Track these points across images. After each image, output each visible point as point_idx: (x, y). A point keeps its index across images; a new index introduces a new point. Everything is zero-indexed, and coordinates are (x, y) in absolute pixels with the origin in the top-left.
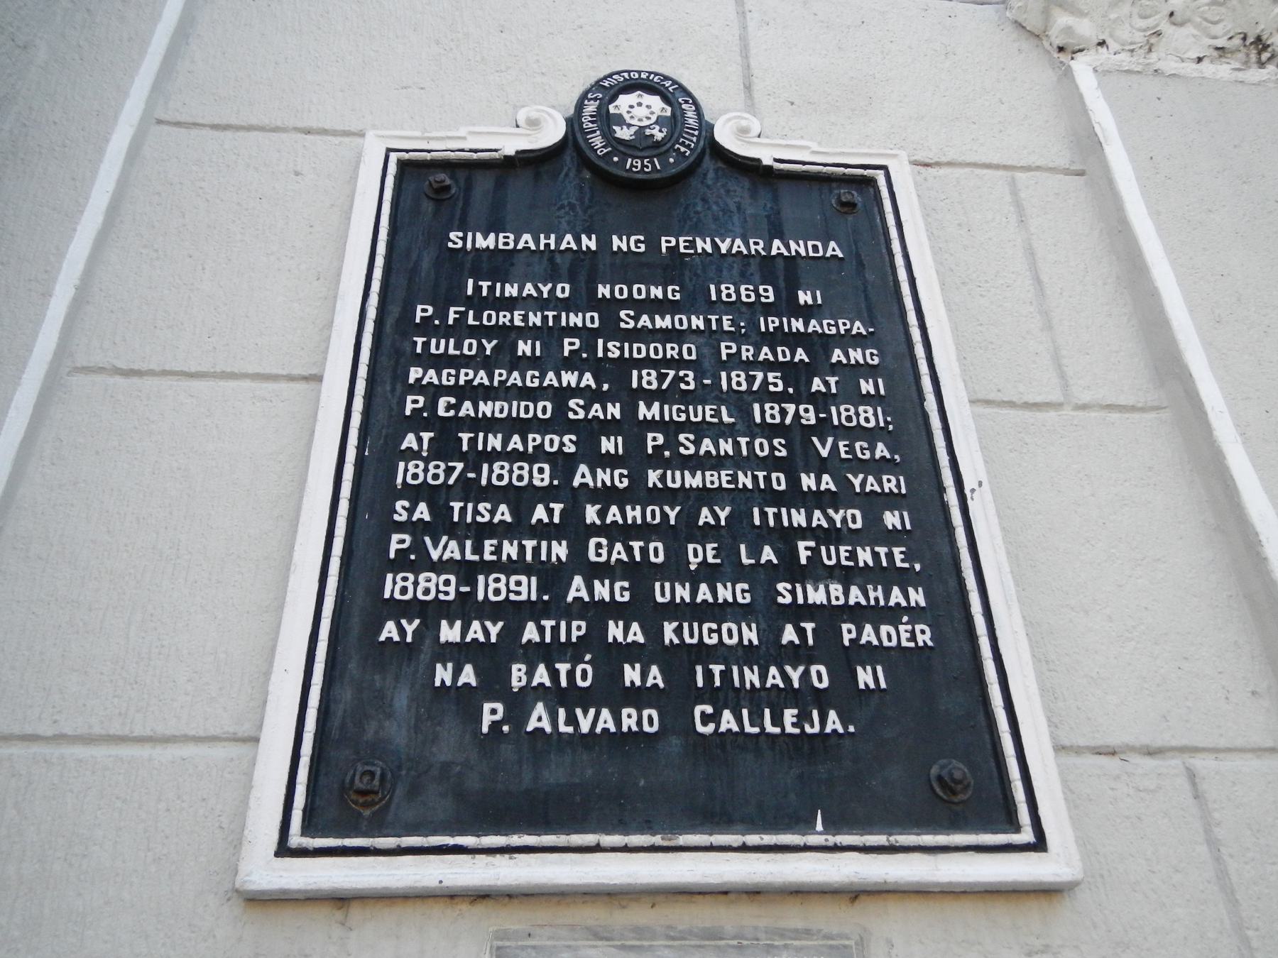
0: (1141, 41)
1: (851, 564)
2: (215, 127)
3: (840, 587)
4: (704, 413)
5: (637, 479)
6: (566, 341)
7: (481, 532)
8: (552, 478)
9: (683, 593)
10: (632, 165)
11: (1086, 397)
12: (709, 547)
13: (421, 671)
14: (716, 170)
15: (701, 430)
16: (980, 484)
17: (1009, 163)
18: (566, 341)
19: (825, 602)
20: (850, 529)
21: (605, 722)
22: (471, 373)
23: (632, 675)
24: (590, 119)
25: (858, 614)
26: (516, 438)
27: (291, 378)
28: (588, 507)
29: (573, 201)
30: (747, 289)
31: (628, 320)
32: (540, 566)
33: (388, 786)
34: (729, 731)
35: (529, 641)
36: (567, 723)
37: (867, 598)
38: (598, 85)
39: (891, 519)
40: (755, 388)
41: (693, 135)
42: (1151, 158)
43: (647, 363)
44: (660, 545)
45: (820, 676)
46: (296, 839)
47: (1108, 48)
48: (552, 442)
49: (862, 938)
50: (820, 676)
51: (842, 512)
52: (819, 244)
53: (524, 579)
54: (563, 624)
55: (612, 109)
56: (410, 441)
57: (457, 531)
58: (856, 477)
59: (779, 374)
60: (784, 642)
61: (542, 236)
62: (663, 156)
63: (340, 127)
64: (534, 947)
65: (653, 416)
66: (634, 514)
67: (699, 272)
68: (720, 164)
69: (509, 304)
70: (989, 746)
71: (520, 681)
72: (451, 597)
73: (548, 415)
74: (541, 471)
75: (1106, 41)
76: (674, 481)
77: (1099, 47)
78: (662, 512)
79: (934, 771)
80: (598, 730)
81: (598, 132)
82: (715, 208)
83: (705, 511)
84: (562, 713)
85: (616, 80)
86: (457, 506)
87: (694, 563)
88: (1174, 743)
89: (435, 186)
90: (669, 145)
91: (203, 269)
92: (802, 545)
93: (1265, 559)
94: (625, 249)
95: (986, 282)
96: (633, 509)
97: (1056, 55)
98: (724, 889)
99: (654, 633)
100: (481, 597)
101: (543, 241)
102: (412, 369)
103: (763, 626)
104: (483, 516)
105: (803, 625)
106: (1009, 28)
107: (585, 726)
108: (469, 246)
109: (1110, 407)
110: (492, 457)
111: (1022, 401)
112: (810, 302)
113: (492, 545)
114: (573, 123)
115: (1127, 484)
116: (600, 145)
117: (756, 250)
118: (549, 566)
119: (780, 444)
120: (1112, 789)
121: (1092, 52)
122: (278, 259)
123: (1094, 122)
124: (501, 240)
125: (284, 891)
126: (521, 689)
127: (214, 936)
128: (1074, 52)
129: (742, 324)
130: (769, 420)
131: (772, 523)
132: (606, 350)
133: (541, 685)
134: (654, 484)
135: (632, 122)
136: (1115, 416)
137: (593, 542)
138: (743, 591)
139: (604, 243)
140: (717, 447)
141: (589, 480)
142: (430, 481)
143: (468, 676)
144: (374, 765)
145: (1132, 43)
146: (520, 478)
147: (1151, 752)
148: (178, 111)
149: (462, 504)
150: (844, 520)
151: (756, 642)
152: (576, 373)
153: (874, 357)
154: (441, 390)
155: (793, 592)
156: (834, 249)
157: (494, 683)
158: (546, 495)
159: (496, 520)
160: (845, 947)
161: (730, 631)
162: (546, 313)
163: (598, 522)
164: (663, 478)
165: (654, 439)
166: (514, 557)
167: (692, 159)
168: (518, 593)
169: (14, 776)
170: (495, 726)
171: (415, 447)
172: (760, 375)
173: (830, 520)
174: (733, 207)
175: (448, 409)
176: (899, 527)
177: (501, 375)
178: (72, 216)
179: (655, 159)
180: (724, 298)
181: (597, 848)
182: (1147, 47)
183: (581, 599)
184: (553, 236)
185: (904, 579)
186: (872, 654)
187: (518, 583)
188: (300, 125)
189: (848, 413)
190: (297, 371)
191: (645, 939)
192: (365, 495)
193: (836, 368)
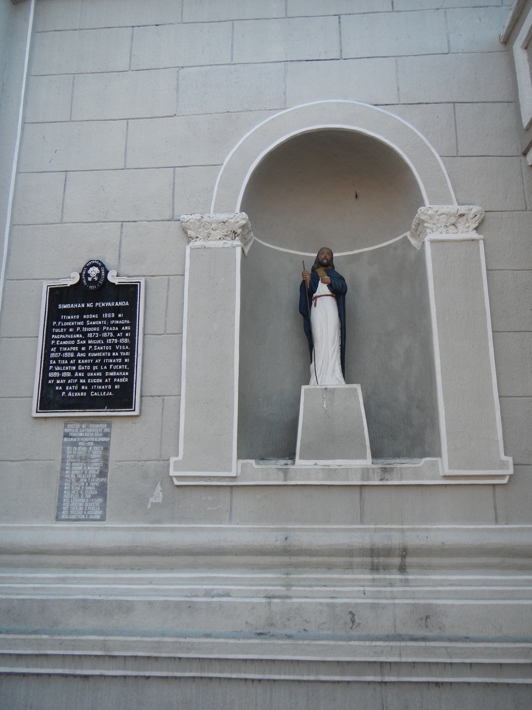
3: (115, 373)
4: (99, 342)
5: (87, 355)
8: (74, 355)
9: (92, 374)
15: (98, 345)
25: (117, 377)
45: (110, 387)
46: (38, 411)
50: (110, 387)
54: (74, 380)
56: (52, 350)
66: (86, 361)
74: (72, 354)
78: (90, 360)
83: (97, 360)
84: (73, 393)
86: (59, 361)
92: (111, 365)
99: (87, 381)
102: (53, 335)
107: (76, 395)
108: (62, 308)
110: (65, 352)
132: (84, 329)
139: (86, 305)
143: (61, 388)
146: (69, 355)
150: (118, 361)
154: (58, 339)
156: (127, 304)
157: (64, 389)
164: (91, 355)
165: (90, 347)
168: (68, 375)
170: (64, 395)
186: (117, 383)
187: (68, 374)
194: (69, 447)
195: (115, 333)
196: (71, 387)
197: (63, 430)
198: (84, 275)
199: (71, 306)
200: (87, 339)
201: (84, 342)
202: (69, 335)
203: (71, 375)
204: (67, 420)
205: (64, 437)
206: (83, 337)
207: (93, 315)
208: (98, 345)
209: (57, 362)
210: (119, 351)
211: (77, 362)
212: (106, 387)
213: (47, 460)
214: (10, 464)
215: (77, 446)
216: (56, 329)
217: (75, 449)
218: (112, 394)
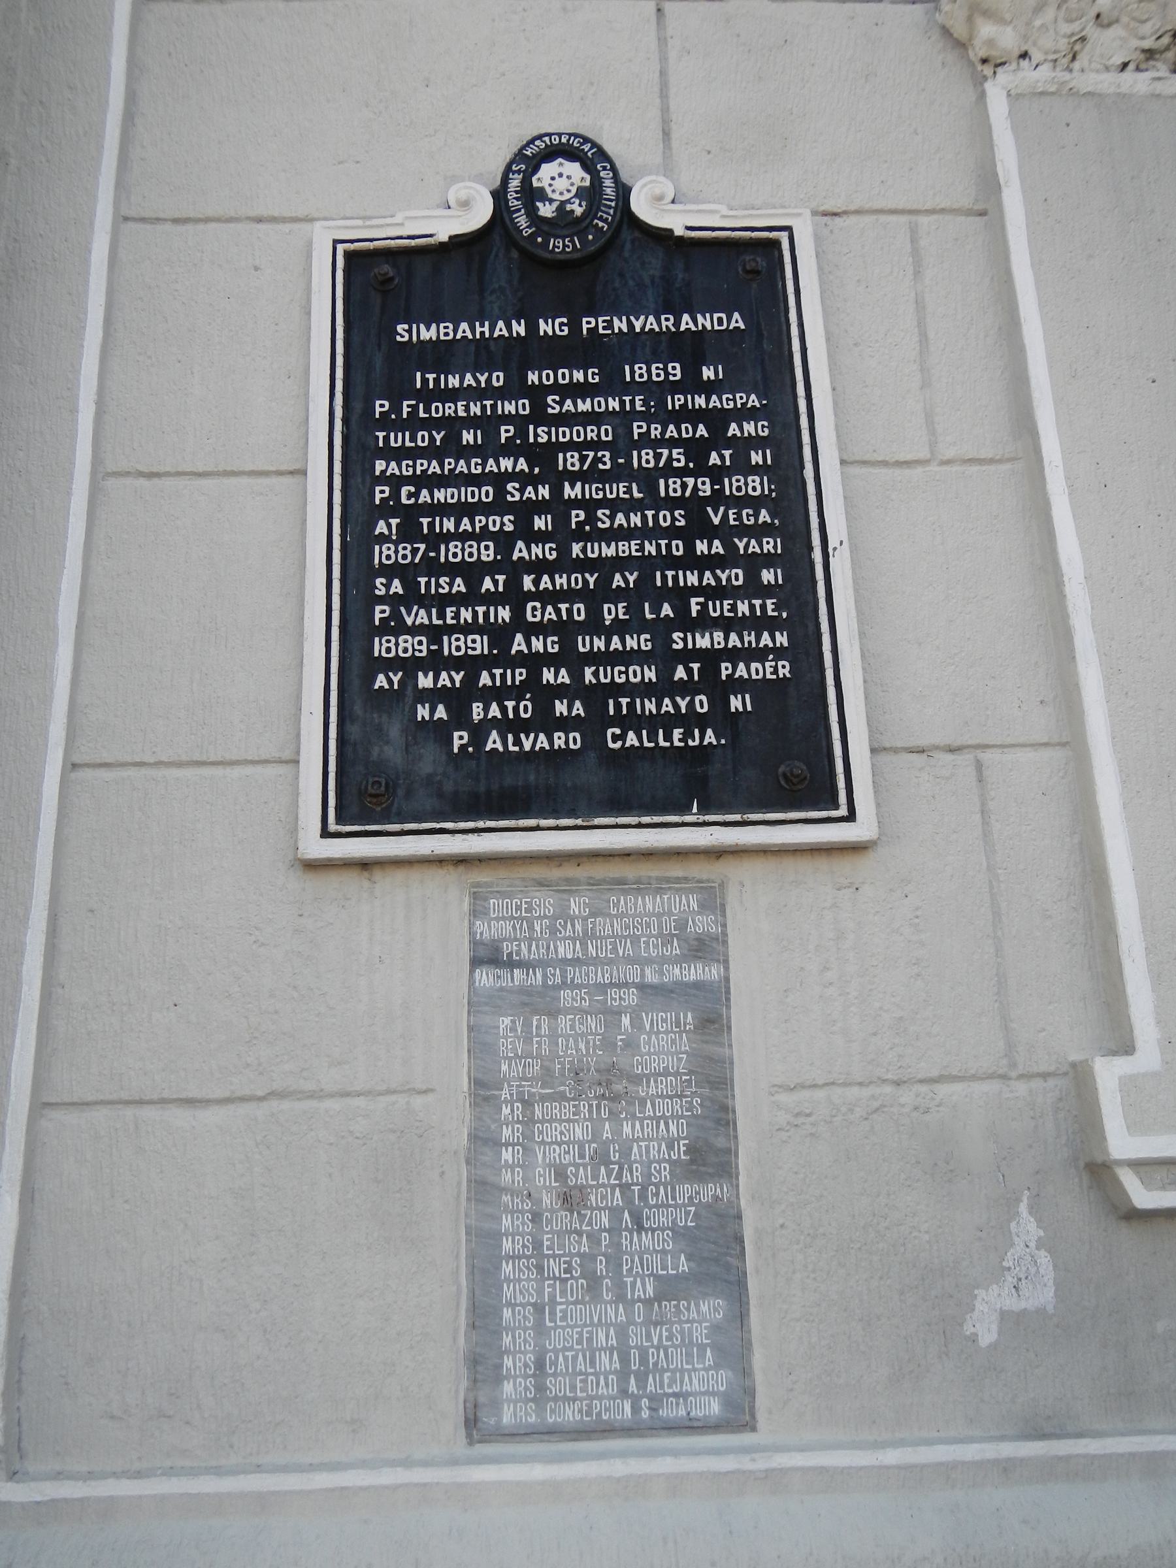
1: (732, 615)
2: (176, 221)
3: (721, 634)
4: (619, 490)
5: (564, 550)
6: (503, 428)
7: (443, 602)
8: (496, 554)
9: (599, 644)
10: (554, 246)
11: (950, 453)
12: (620, 606)
14: (633, 241)
15: (615, 506)
16: (841, 543)
17: (915, 207)
18: (503, 428)
19: (709, 647)
21: (542, 743)
22: (425, 462)
23: (561, 708)
25: (734, 655)
26: (466, 520)
27: (280, 473)
28: (525, 577)
29: (503, 284)
30: (657, 368)
32: (489, 627)
33: (391, 791)
34: (632, 746)
35: (484, 685)
36: (514, 745)
37: (742, 642)
38: (519, 156)
39: (767, 576)
40: (661, 465)
41: (610, 207)
43: (571, 446)
44: (582, 606)
45: (702, 704)
47: (1030, 59)
48: (494, 523)
49: (723, 882)
50: (702, 704)
51: (727, 571)
52: (724, 316)
53: (478, 637)
54: (509, 671)
55: (535, 184)
56: (381, 528)
57: (425, 601)
59: (681, 450)
60: (676, 679)
61: (477, 324)
62: (582, 234)
63: (287, 214)
64: (497, 892)
65: (576, 495)
66: (561, 581)
68: (637, 234)
69: (452, 395)
70: (825, 750)
71: (479, 715)
72: (424, 654)
73: (490, 499)
74: (487, 548)
75: (1029, 52)
76: (593, 552)
77: (1021, 60)
78: (583, 577)
79: (781, 769)
80: (537, 748)
81: (523, 211)
82: (631, 283)
83: (618, 576)
85: (538, 147)
86: (423, 580)
87: (608, 619)
88: (970, 742)
90: (588, 221)
91: (192, 373)
92: (693, 601)
93: (1065, 596)
94: (550, 333)
95: (877, 341)
96: (561, 577)
97: (980, 67)
98: (626, 852)
99: (576, 675)
100: (446, 653)
101: (478, 330)
102: (377, 462)
103: (661, 667)
104: (444, 588)
105: (691, 665)
107: (527, 746)
108: (415, 338)
110: (448, 537)
111: (894, 460)
112: (712, 377)
113: (452, 612)
114: (499, 195)
115: (973, 532)
116: (525, 225)
117: (667, 326)
118: (497, 626)
119: (680, 515)
120: (916, 777)
121: (1014, 66)
122: (253, 360)
123: (997, 160)
124: (442, 331)
126: (480, 720)
127: (287, 888)
128: (997, 66)
129: (652, 403)
130: (672, 494)
131: (670, 584)
132: (536, 435)
134: (577, 555)
135: (556, 196)
136: (975, 468)
137: (530, 605)
138: (646, 640)
139: (532, 328)
141: (525, 554)
142: (400, 561)
143: (441, 712)
144: (379, 777)
145: (1055, 52)
146: (471, 555)
147: (952, 750)
149: (426, 579)
150: (729, 579)
151: (654, 680)
153: (765, 429)
155: (685, 640)
156: (737, 321)
157: (460, 717)
158: (491, 569)
159: (454, 591)
160: (711, 887)
161: (635, 673)
163: (533, 589)
164: (584, 550)
166: (470, 621)
168: (474, 649)
169: (134, 790)
170: (463, 748)
171: (386, 533)
172: (665, 452)
173: (718, 579)
174: (647, 281)
176: (773, 583)
177: (450, 464)
178: (78, 332)
179: (576, 238)
180: (637, 379)
182: (1071, 55)
183: (522, 651)
184: (487, 323)
185: (772, 625)
187: (474, 641)
188: (252, 214)
189: (739, 484)
190: (284, 468)
191: (574, 886)
192: (352, 575)
193: (732, 442)
194: (507, 1021)
195: (696, 450)
196: (494, 706)
197: (466, 929)
198: (516, 192)
199: (460, 330)
200: (558, 479)
201: (544, 492)
202: (462, 462)
203: (490, 650)
204: (483, 876)
205: (476, 962)
206: (537, 470)
207: (575, 372)
208: (615, 506)
209: (410, 585)
210: (724, 532)
211: (514, 583)
212: (683, 704)
213: (389, 1092)
215: (553, 1013)
216: (392, 435)
217: (538, 1027)
218: (718, 738)
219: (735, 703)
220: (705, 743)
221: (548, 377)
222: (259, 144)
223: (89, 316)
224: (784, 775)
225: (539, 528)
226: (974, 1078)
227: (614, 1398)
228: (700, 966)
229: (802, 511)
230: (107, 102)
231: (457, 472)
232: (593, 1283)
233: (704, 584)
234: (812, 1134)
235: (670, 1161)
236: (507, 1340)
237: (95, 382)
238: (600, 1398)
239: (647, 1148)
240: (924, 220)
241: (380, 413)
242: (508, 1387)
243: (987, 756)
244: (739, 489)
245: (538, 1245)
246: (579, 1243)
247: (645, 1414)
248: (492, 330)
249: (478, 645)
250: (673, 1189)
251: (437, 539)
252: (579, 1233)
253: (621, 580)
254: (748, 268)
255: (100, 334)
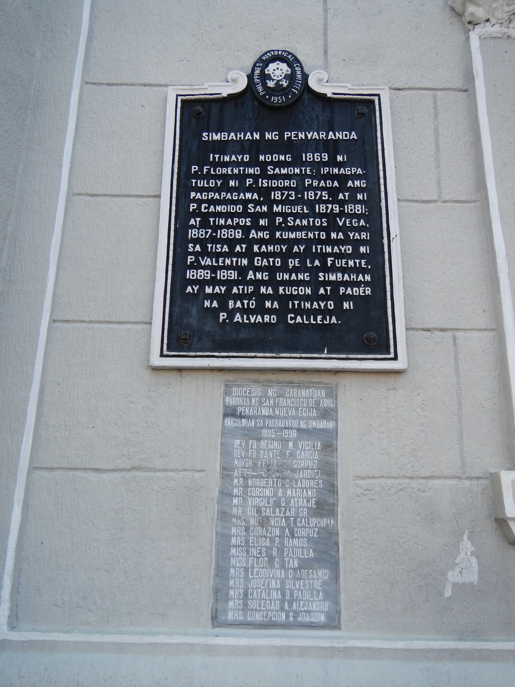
0: (506, 17)
1: (346, 266)
2: (108, 84)
3: (341, 274)
4: (298, 209)
5: (272, 235)
6: (248, 180)
7: (218, 255)
8: (242, 235)
9: (286, 277)
10: (274, 100)
11: (447, 198)
12: (296, 260)
13: (200, 302)
14: (309, 99)
15: (296, 216)
17: (435, 87)
18: (248, 180)
19: (335, 280)
20: (347, 253)
22: (213, 194)
23: (268, 304)
24: (257, 77)
25: (346, 284)
26: (229, 220)
27: (149, 196)
28: (255, 246)
29: (250, 116)
30: (317, 155)
31: (271, 170)
32: (238, 267)
33: (192, 338)
36: (247, 320)
37: (350, 278)
38: (260, 60)
39: (362, 249)
40: (317, 198)
41: (299, 83)
42: (495, 85)
43: (278, 188)
44: (279, 260)
45: (331, 305)
47: (490, 22)
48: (242, 222)
49: (337, 385)
50: (331, 305)
51: (345, 247)
52: (348, 133)
54: (246, 287)
55: (266, 72)
56: (192, 222)
57: (211, 255)
58: (351, 233)
59: (326, 192)
60: (320, 293)
61: (238, 133)
63: (157, 83)
64: (236, 384)
65: (279, 211)
66: (271, 248)
67: (299, 148)
68: (311, 96)
69: (226, 165)
70: (385, 328)
72: (209, 278)
73: (241, 211)
74: (238, 232)
75: (490, 19)
76: (285, 236)
77: (486, 22)
79: (365, 335)
80: (257, 322)
81: (260, 84)
82: (307, 117)
83: (296, 247)
84: (245, 316)
85: (268, 56)
86: (209, 246)
87: (291, 266)
88: (451, 327)
89: (197, 112)
90: (289, 89)
91: (113, 151)
92: (329, 259)
94: (270, 139)
95: (416, 147)
96: (270, 246)
97: (467, 26)
99: (276, 290)
100: (218, 278)
101: (239, 136)
102: (192, 193)
103: (313, 288)
105: (327, 288)
106: (448, 11)
107: (252, 321)
108: (210, 139)
109: (456, 201)
110: (221, 227)
112: (342, 160)
114: (250, 77)
115: (456, 233)
116: (261, 90)
117: (322, 137)
119: (325, 221)
121: (482, 25)
122: (139, 146)
124: (223, 136)
125: (163, 367)
126: (232, 308)
129: (314, 171)
130: (321, 211)
131: (319, 251)
132: (262, 183)
133: (238, 307)
135: (275, 78)
136: (458, 205)
137: (256, 258)
138: (307, 276)
139: (262, 136)
140: (301, 222)
141: (255, 236)
143: (215, 304)
144: (187, 331)
145: (502, 19)
146: (231, 235)
147: (442, 330)
148: (93, 77)
149: (211, 245)
150: (345, 250)
151: (310, 293)
152: (251, 193)
153: (364, 184)
154: (202, 201)
155: (324, 276)
156: (354, 136)
157: (223, 307)
158: (240, 242)
159: (223, 251)
160: (331, 387)
161: (302, 290)
162: (240, 168)
163: (258, 251)
164: (281, 235)
165: (279, 220)
166: (230, 264)
167: (298, 95)
168: (231, 277)
170: (224, 320)
171: (194, 224)
172: (319, 193)
173: (340, 250)
174: (314, 117)
175: (205, 208)
176: (365, 252)
177: (224, 195)
180: (308, 160)
181: (255, 357)
182: (509, 21)
183: (252, 279)
184: (242, 133)
185: (364, 271)
187: (231, 273)
188: (141, 82)
190: (151, 194)
193: (349, 189)
194: (238, 441)
195: (333, 192)
196: (239, 302)
197: (222, 400)
198: (258, 76)
199: (231, 136)
200: (271, 203)
201: (265, 208)
202: (229, 194)
203: (238, 277)
204: (230, 377)
205: (226, 415)
206: (262, 199)
207: (280, 156)
208: (296, 216)
209: (204, 248)
210: (344, 229)
211: (250, 248)
212: (322, 305)
213: (185, 470)
214: (93, 477)
215: (259, 439)
216: (199, 181)
217: (252, 445)
218: (337, 321)
219: (346, 305)
220: (332, 322)
221: (269, 158)
222: (146, 52)
223: (69, 124)
224: (366, 338)
225: (262, 225)
226: (446, 477)
227: (278, 611)
228: (325, 422)
229: (379, 221)
230: (80, 32)
231: (226, 198)
232: (271, 560)
233: (334, 252)
234: (372, 499)
235: (308, 508)
236: (232, 582)
237: (70, 154)
238: (272, 611)
239: (298, 501)
240: (439, 93)
241: (194, 171)
242: (231, 604)
243: (458, 334)
244: (351, 210)
245: (247, 541)
246: (266, 541)
247: (291, 619)
248: (245, 136)
249: (233, 275)
250: (308, 520)
251: (216, 228)
252: (266, 537)
253: (297, 249)
254: (360, 112)
255: (73, 132)
